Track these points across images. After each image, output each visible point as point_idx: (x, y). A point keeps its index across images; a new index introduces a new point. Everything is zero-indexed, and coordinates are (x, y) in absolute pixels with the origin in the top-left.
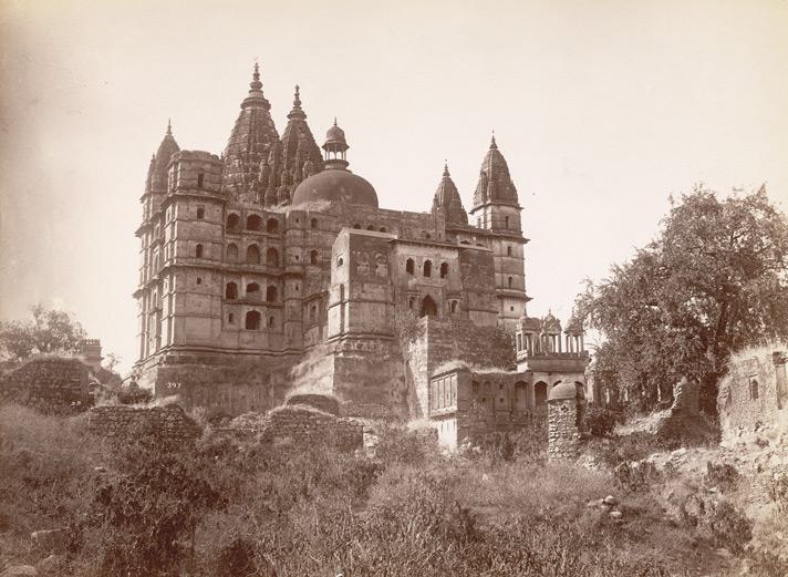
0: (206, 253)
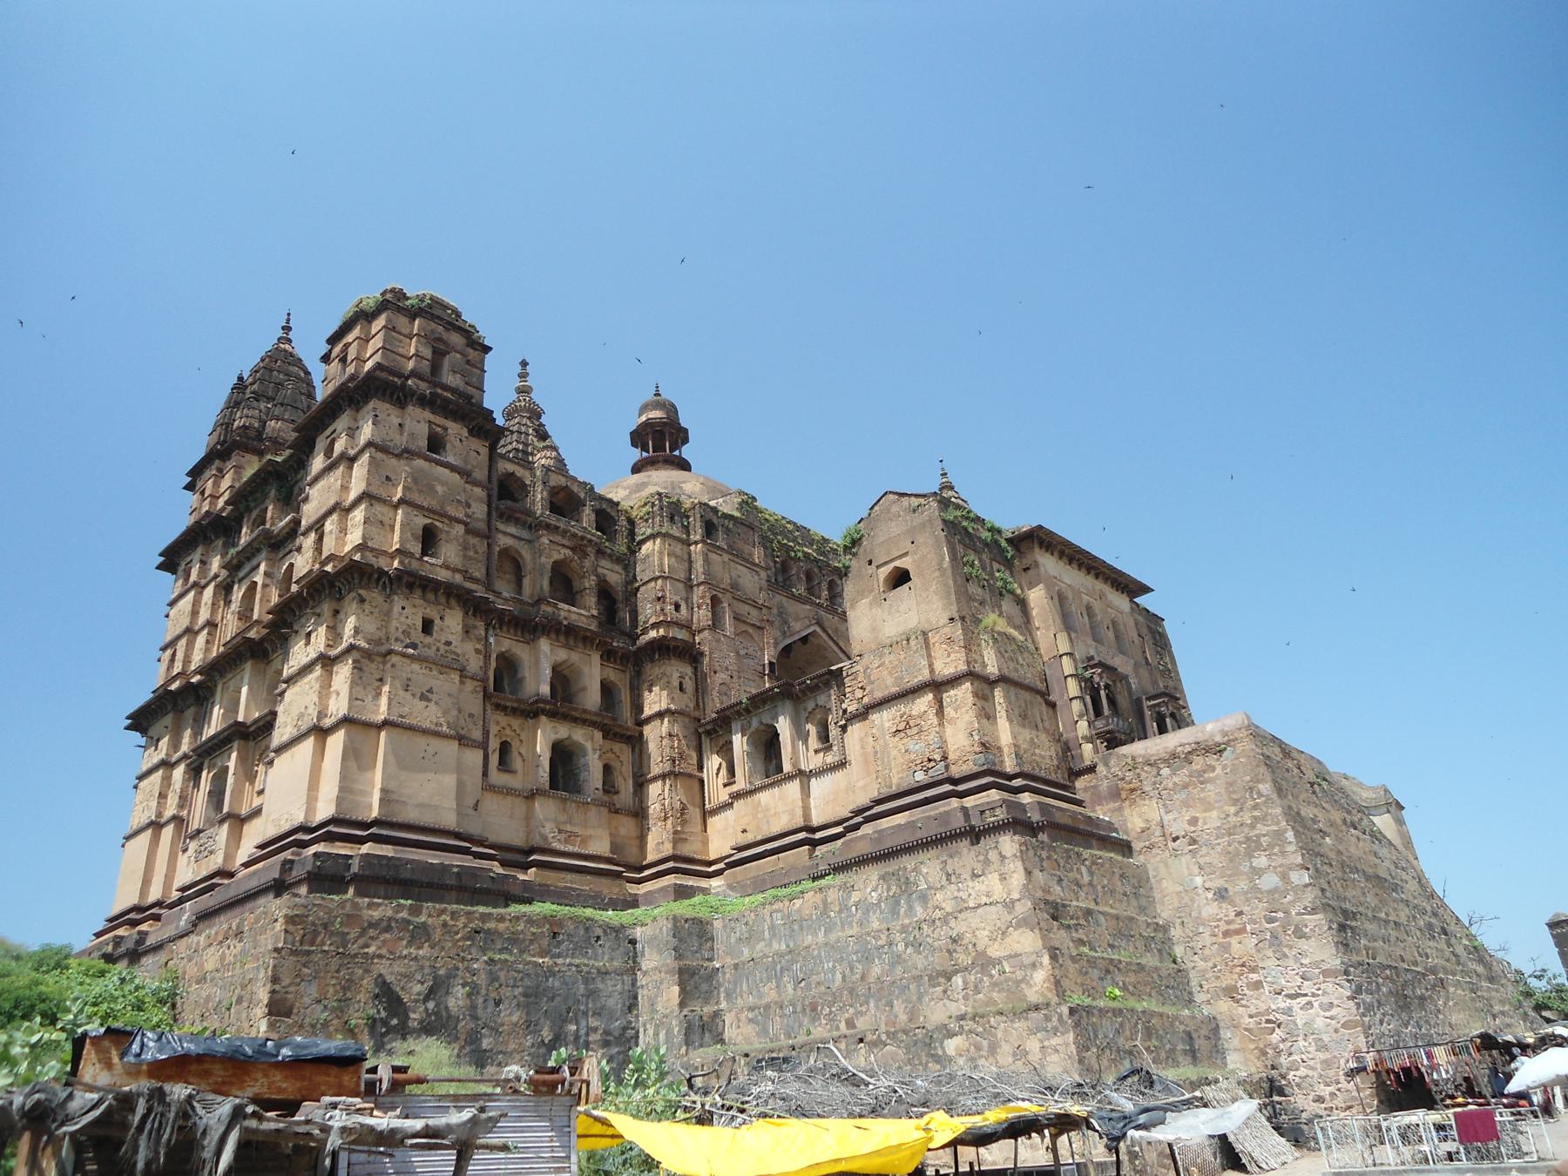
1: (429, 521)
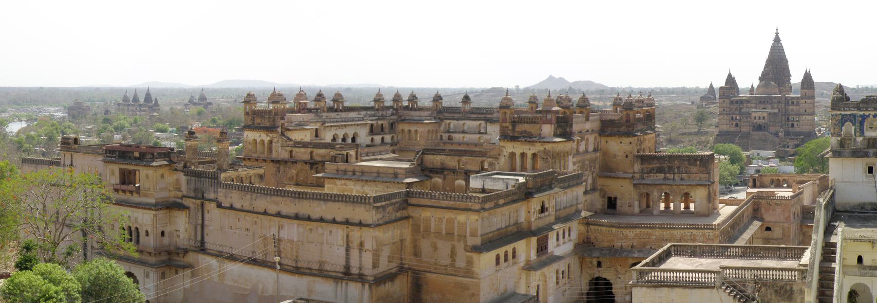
0: (725, 110)
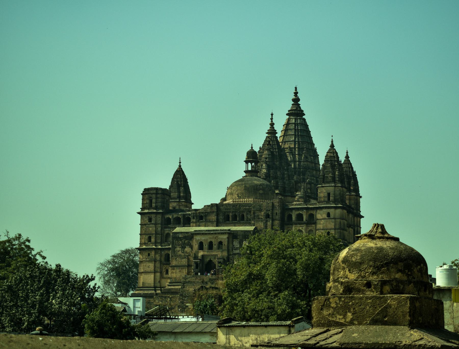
0: (153, 240)
1: (149, 236)
